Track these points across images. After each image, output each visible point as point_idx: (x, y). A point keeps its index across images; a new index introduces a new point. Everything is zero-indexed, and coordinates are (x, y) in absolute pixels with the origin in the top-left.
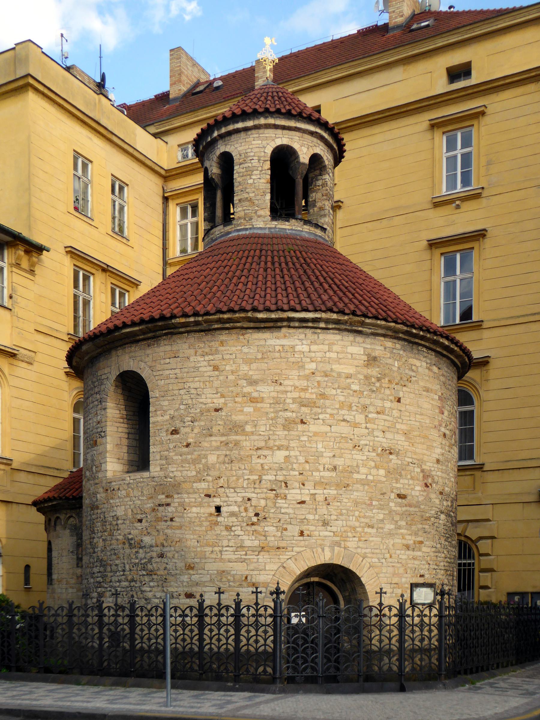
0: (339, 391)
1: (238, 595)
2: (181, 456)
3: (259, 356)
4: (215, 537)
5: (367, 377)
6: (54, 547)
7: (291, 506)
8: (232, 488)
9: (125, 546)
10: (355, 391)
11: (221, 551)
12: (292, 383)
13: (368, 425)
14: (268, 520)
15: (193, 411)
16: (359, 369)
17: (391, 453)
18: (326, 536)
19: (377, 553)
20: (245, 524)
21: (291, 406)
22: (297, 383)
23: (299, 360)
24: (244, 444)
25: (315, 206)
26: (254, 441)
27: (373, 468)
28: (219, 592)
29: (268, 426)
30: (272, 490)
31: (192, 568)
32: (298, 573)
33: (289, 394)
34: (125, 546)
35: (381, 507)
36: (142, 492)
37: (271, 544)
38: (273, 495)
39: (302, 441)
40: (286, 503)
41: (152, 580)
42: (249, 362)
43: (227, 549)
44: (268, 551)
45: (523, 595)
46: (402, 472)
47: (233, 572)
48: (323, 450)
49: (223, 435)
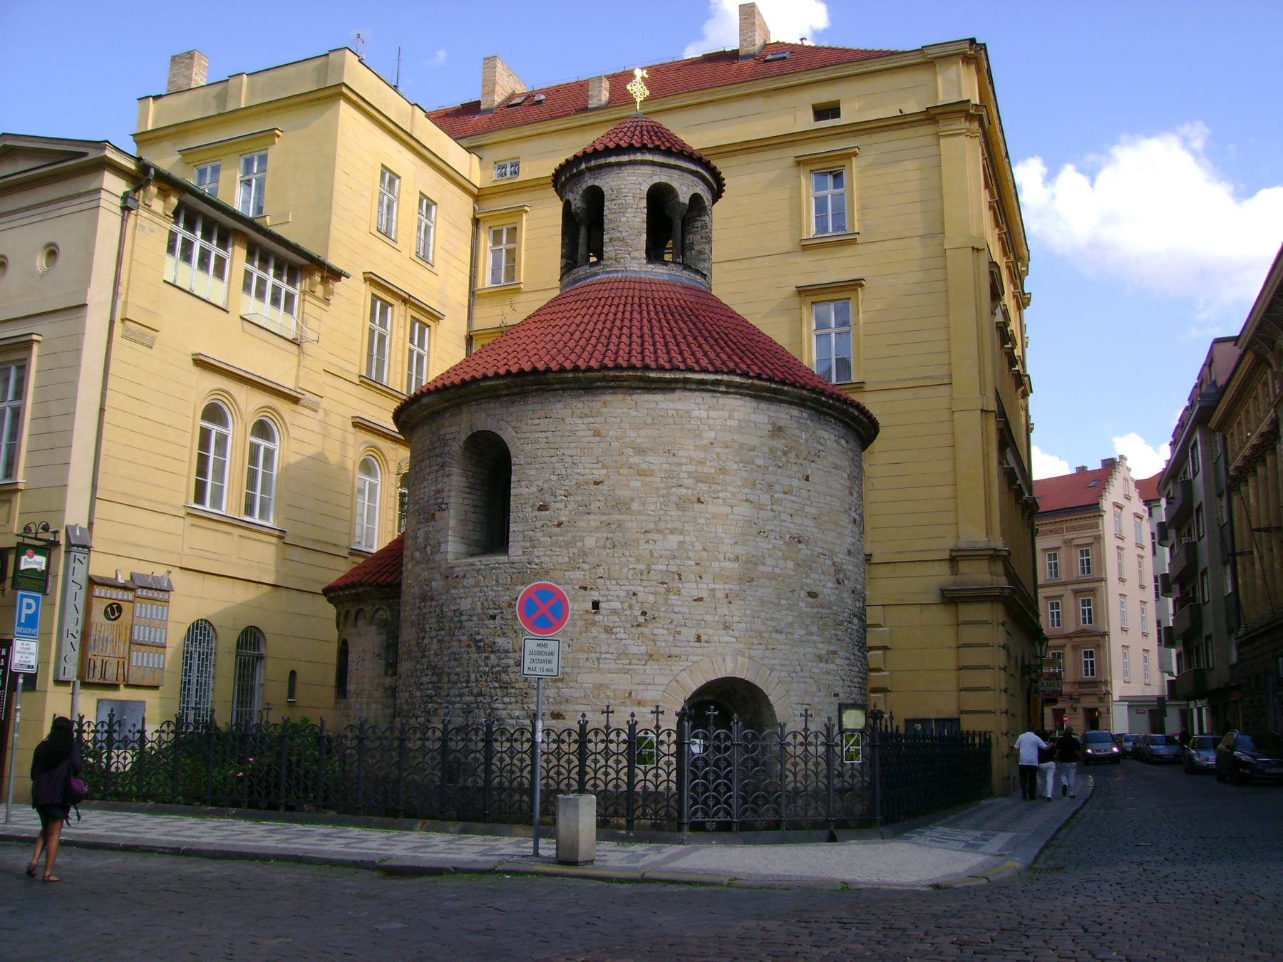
1: (633, 715)
2: (550, 537)
3: (649, 421)
4: (591, 641)
5: (772, 451)
6: (351, 649)
7: (686, 604)
8: (614, 579)
9: (470, 650)
10: (759, 467)
11: (598, 659)
12: (687, 455)
13: (774, 507)
14: (658, 620)
15: (567, 482)
16: (763, 440)
17: (799, 542)
18: (727, 643)
20: (629, 625)
21: (686, 481)
22: (693, 454)
24: (630, 525)
25: (693, 249)
26: (642, 521)
28: (608, 712)
29: (658, 505)
30: (663, 583)
31: (561, 680)
32: (695, 688)
33: (684, 468)
34: (470, 650)
36: (497, 581)
37: (662, 651)
40: (679, 600)
41: (507, 695)
42: (636, 427)
43: (607, 656)
44: (658, 660)
45: (925, 721)
46: (813, 565)
47: (613, 687)
48: (724, 535)
49: (604, 514)
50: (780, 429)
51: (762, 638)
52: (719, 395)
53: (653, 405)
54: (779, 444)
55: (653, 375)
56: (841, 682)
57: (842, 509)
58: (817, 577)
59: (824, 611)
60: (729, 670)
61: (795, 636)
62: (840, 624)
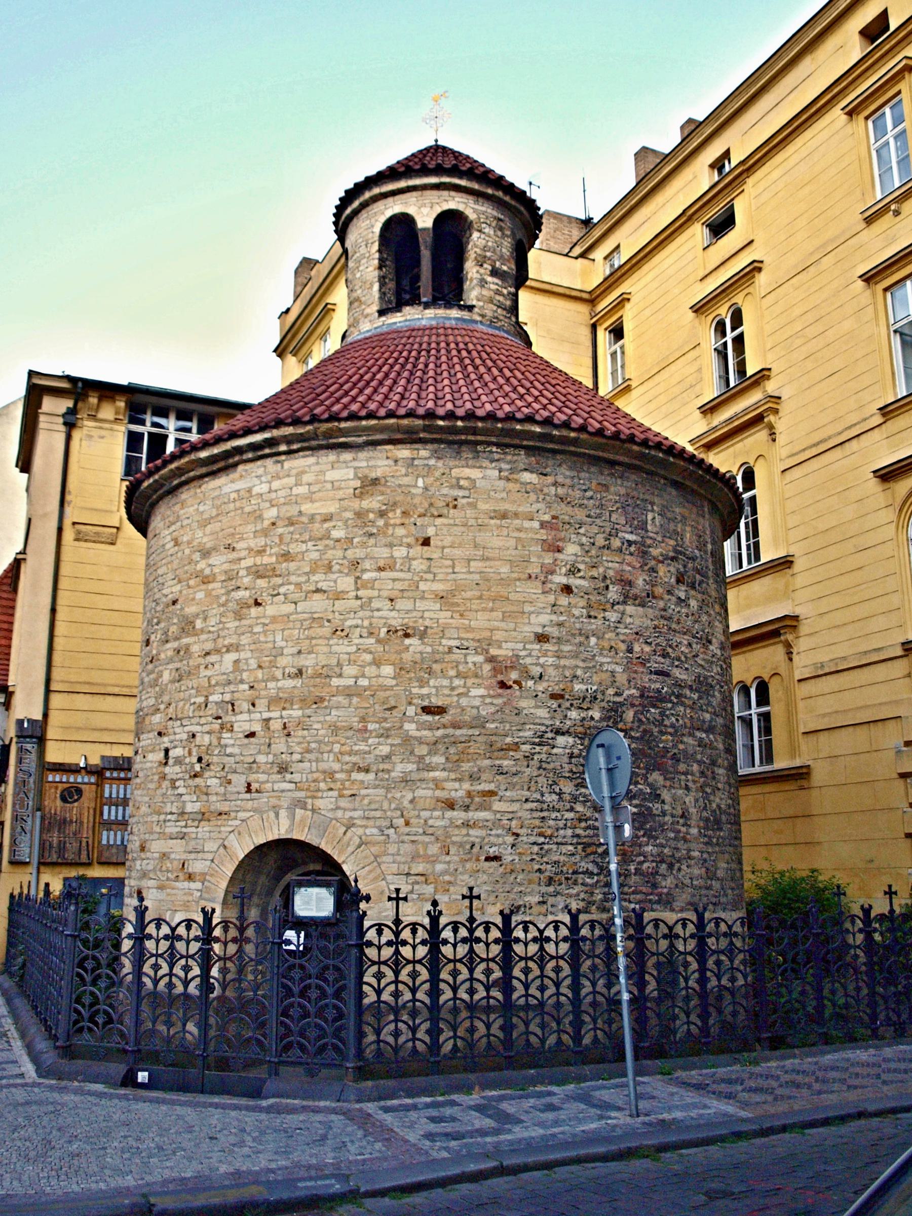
0: (310, 544)
3: (214, 513)
10: (338, 540)
13: (360, 593)
14: (212, 767)
15: (158, 608)
16: (345, 503)
17: (407, 635)
18: (283, 791)
19: (375, 818)
20: (187, 777)
22: (252, 545)
23: (256, 507)
27: (370, 664)
32: (241, 856)
33: (243, 562)
35: (385, 734)
37: (212, 808)
38: (218, 727)
39: (255, 634)
42: (204, 524)
43: (169, 817)
46: (435, 666)
47: (173, 856)
48: (283, 644)
49: (177, 639)
50: (375, 482)
51: (334, 781)
52: (283, 457)
53: (217, 493)
54: (373, 503)
55: (203, 454)
56: (510, 839)
57: (515, 575)
58: (446, 682)
59: (458, 732)
60: (283, 831)
61: (393, 774)
62: (516, 746)
